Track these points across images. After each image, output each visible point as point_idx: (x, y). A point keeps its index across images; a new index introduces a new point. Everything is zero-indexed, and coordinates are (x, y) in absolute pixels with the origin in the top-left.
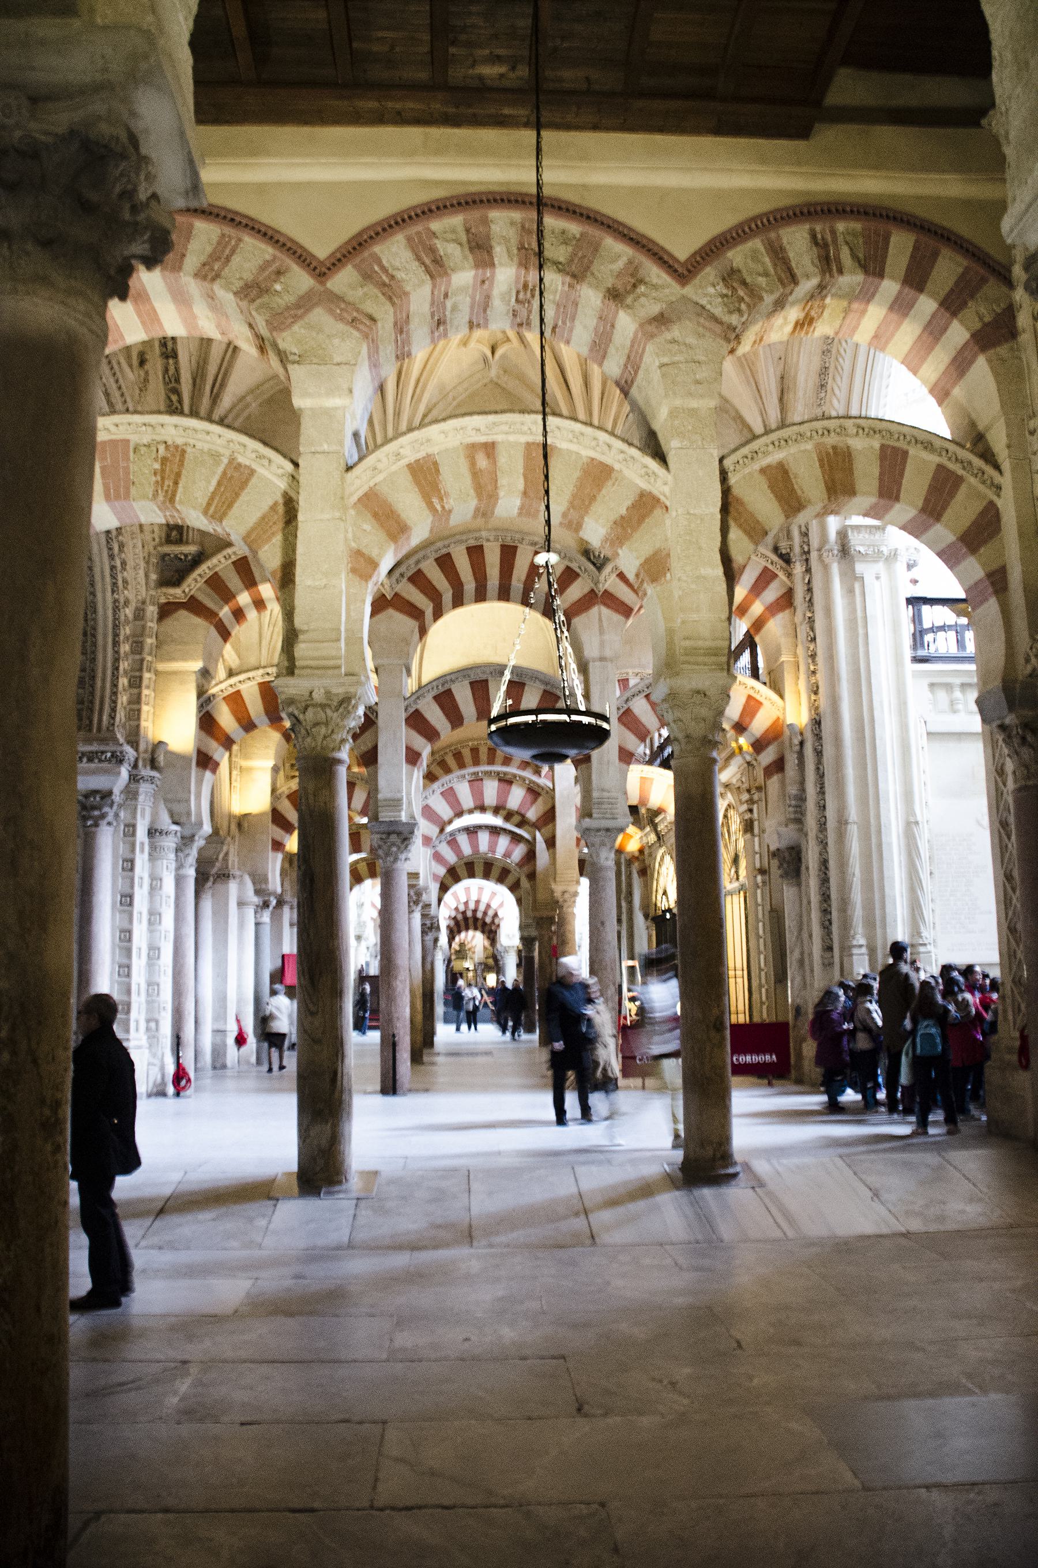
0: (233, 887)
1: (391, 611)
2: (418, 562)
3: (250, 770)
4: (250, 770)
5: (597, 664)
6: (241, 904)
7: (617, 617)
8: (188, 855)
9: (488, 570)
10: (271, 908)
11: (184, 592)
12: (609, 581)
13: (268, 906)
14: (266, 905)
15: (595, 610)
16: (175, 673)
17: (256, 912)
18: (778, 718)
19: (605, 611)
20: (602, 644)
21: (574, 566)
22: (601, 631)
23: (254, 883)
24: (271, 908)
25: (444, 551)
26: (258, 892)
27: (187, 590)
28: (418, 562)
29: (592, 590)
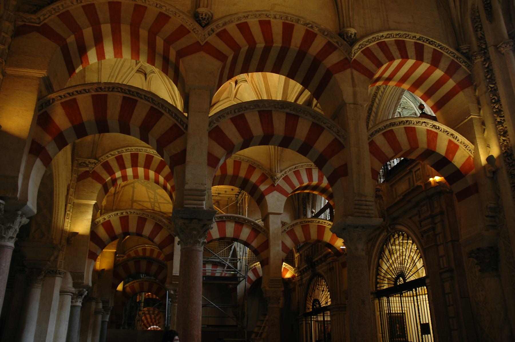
0: (58, 281)
1: (203, 53)
2: (225, 24)
3: (80, 205)
4: (80, 205)
5: (352, 106)
6: (62, 292)
7: (363, 77)
8: (10, 228)
9: (274, 36)
10: (83, 296)
11: (39, 18)
12: (357, 53)
13: (81, 296)
14: (80, 294)
15: (348, 71)
16: (22, 77)
17: (72, 299)
18: (470, 156)
19: (356, 73)
20: (355, 94)
21: (333, 41)
22: (354, 85)
23: (73, 279)
24: (83, 296)
25: (243, 21)
26: (75, 285)
27: (42, 18)
28: (225, 24)
29: (346, 59)
